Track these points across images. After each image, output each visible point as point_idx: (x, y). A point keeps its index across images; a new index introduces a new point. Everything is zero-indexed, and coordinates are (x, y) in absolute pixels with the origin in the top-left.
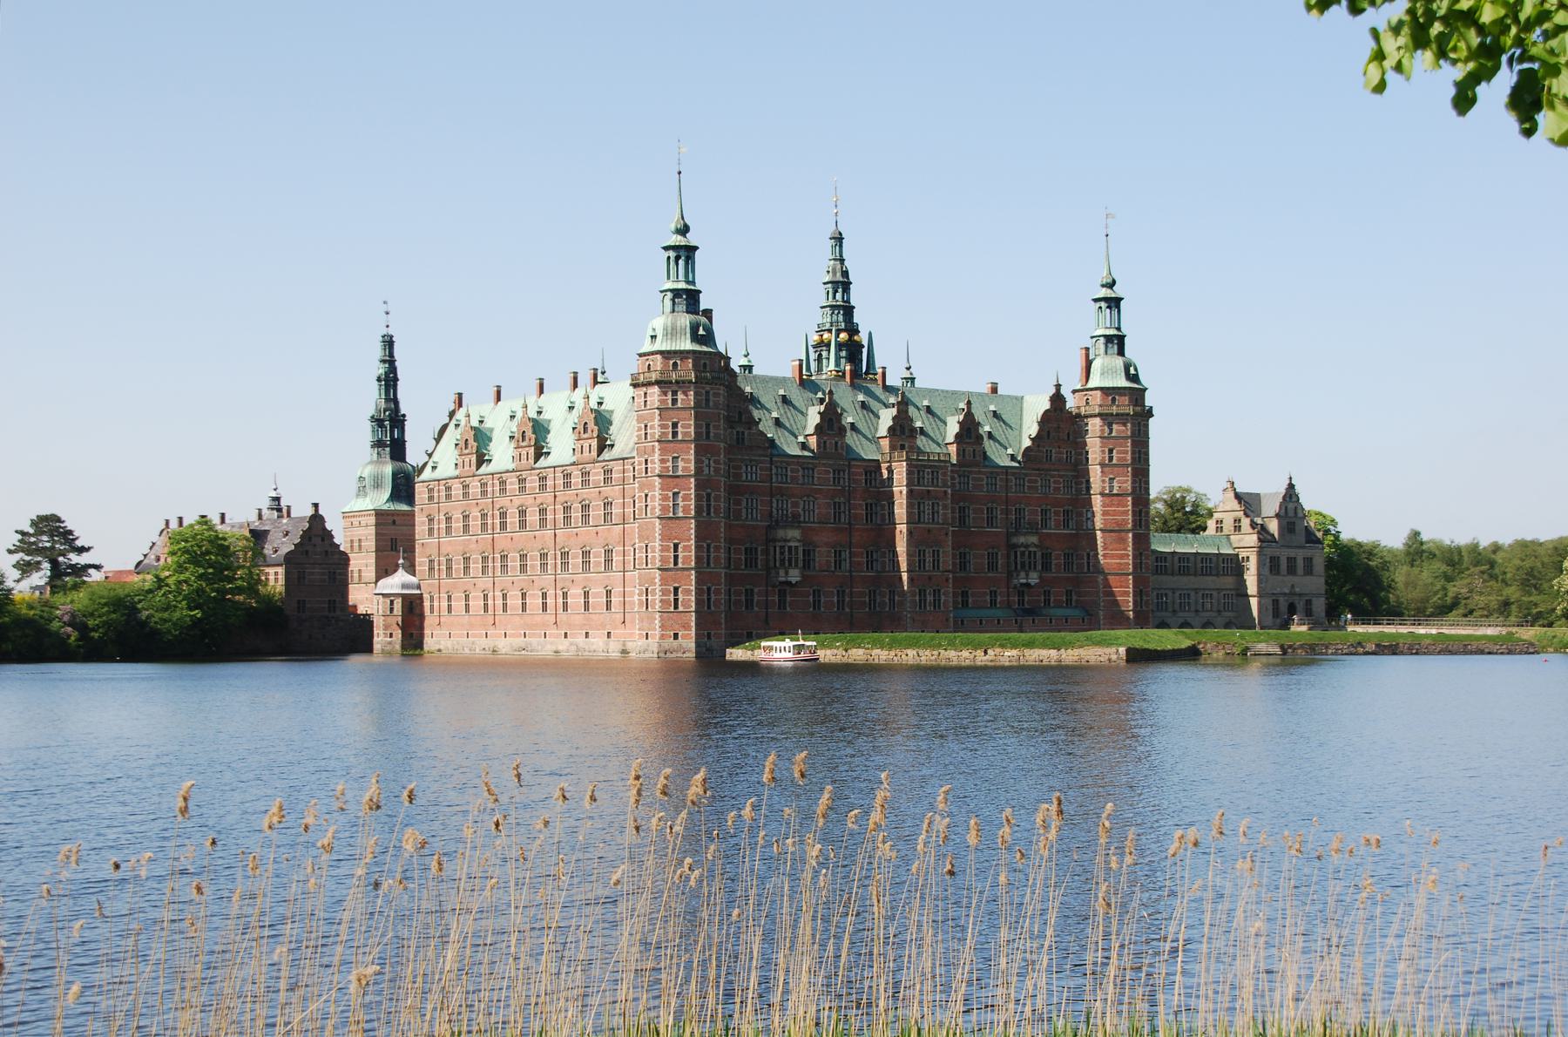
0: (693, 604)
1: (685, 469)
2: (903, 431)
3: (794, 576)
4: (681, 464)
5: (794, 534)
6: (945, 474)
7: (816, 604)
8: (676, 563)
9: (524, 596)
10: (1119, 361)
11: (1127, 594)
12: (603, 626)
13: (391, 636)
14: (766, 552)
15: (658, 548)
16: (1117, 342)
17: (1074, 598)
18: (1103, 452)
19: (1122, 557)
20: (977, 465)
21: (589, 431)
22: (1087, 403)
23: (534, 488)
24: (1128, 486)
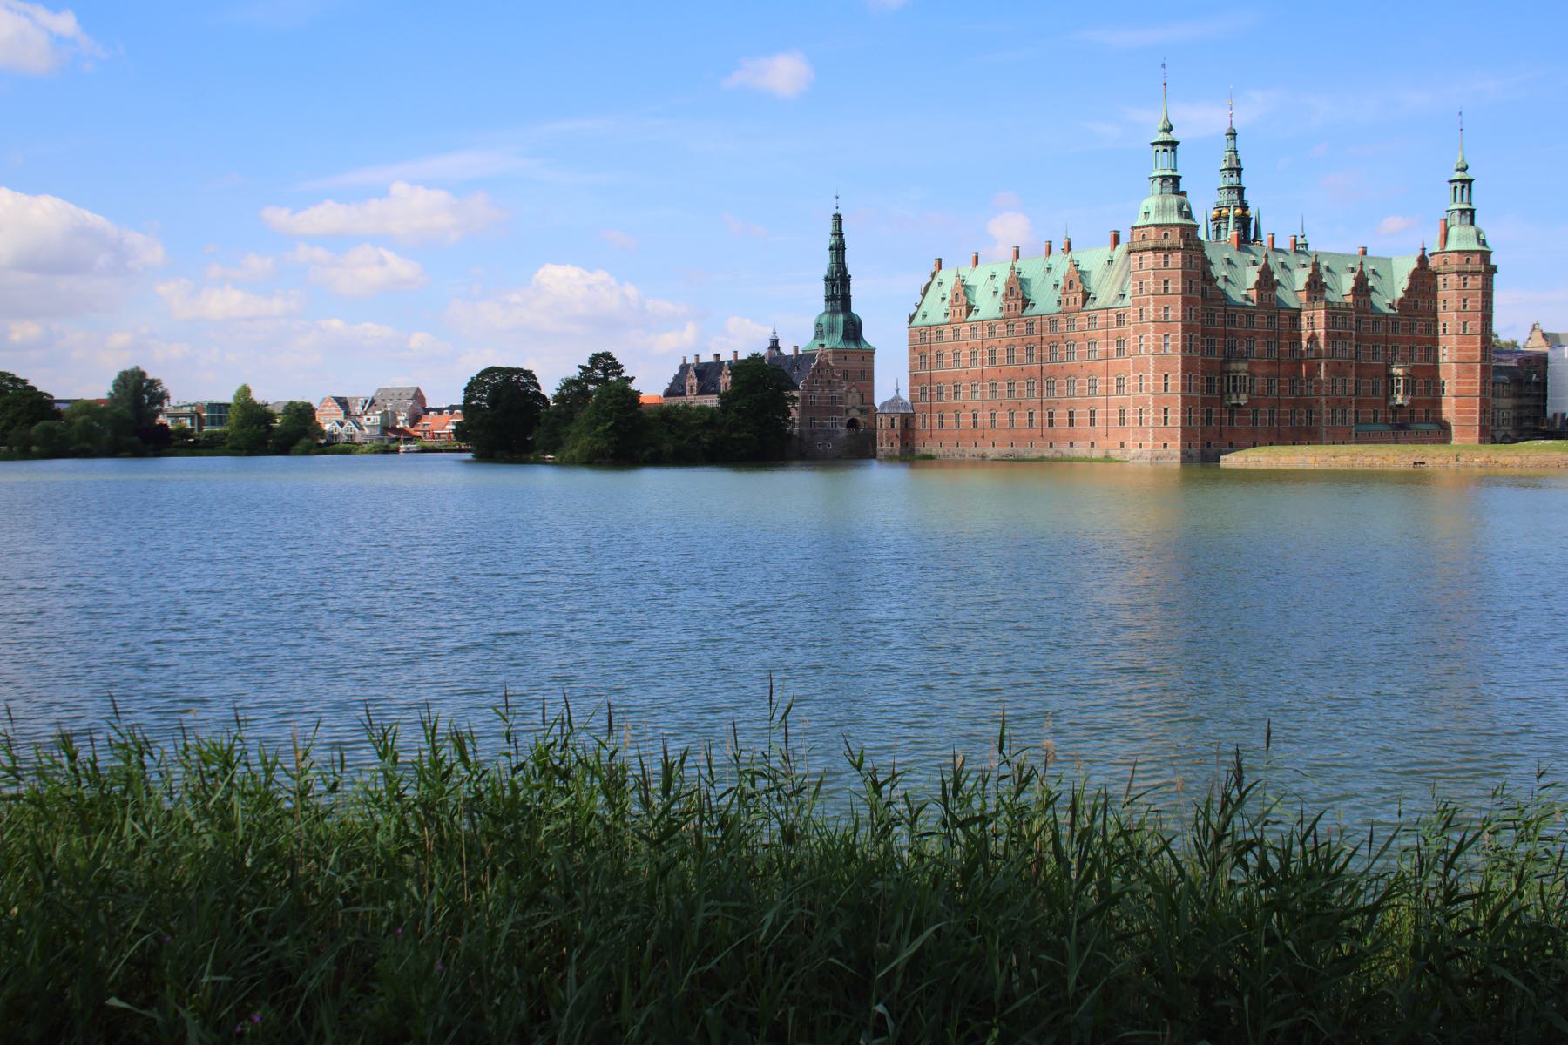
0: (1179, 422)
1: (1174, 316)
2: (1316, 286)
3: (1243, 400)
4: (1170, 313)
5: (1243, 366)
6: (1351, 319)
7: (1255, 421)
8: (1166, 389)
9: (1011, 414)
10: (1472, 230)
11: (1474, 412)
12: (1086, 438)
13: (892, 445)
14: (1221, 381)
15: (1151, 377)
16: (1469, 214)
17: (1431, 416)
18: (1459, 301)
19: (1471, 383)
20: (1366, 312)
21: (1075, 286)
22: (1446, 263)
23: (1023, 332)
24: (1478, 328)
